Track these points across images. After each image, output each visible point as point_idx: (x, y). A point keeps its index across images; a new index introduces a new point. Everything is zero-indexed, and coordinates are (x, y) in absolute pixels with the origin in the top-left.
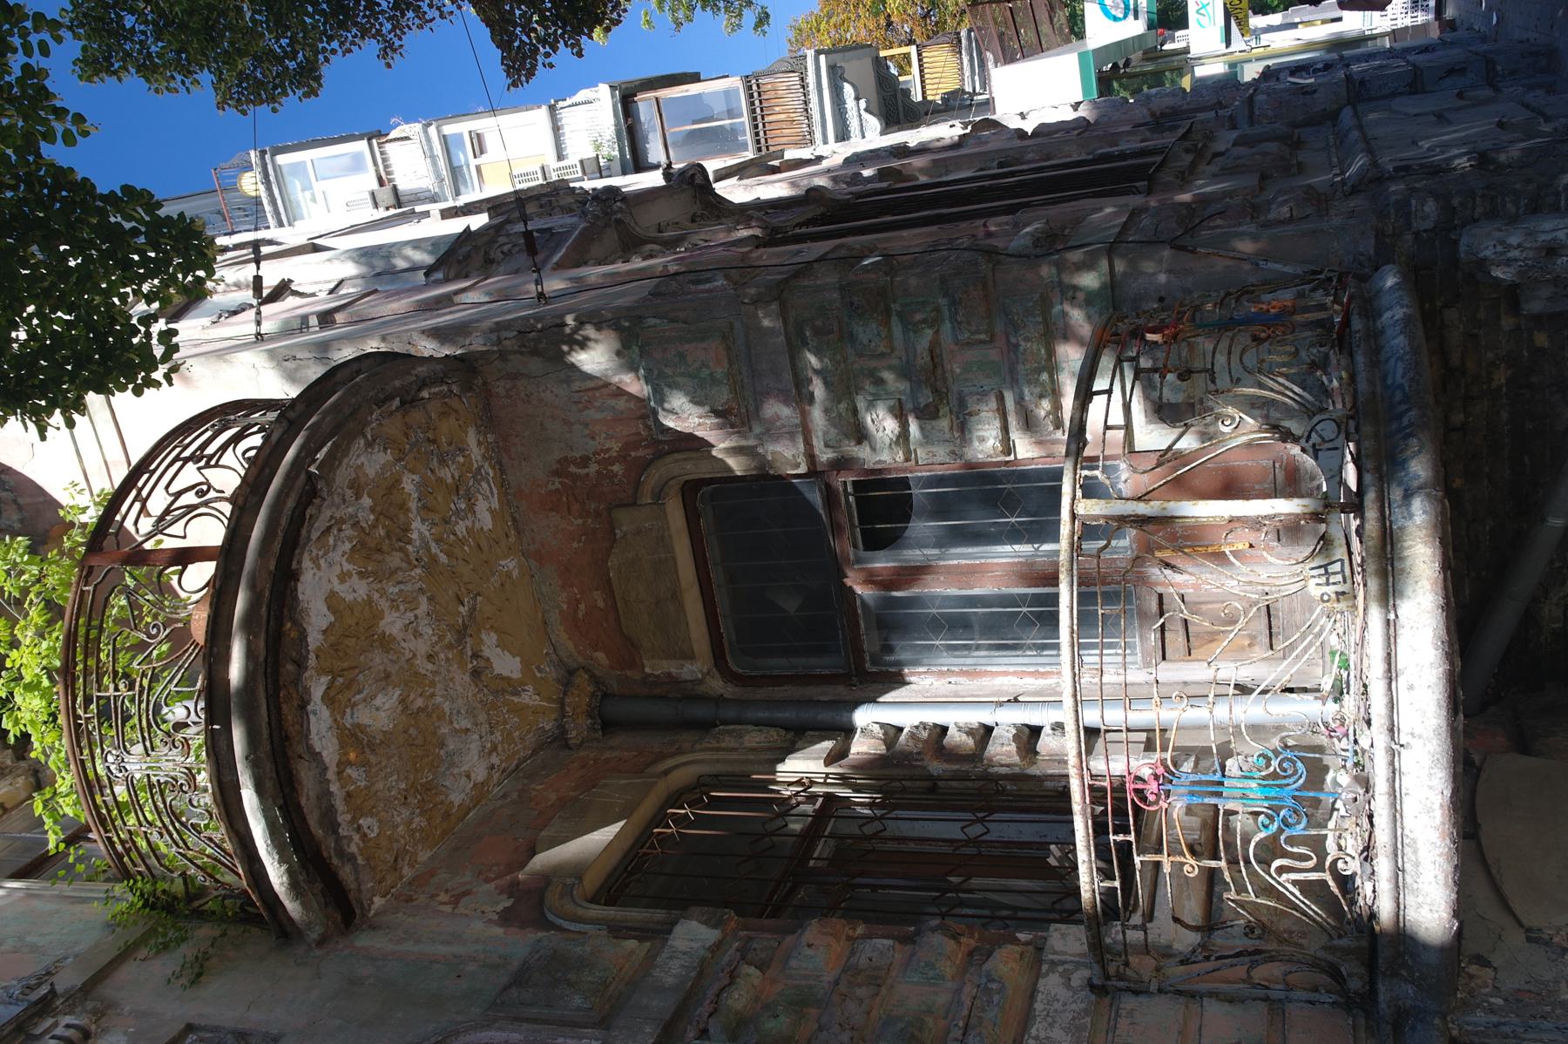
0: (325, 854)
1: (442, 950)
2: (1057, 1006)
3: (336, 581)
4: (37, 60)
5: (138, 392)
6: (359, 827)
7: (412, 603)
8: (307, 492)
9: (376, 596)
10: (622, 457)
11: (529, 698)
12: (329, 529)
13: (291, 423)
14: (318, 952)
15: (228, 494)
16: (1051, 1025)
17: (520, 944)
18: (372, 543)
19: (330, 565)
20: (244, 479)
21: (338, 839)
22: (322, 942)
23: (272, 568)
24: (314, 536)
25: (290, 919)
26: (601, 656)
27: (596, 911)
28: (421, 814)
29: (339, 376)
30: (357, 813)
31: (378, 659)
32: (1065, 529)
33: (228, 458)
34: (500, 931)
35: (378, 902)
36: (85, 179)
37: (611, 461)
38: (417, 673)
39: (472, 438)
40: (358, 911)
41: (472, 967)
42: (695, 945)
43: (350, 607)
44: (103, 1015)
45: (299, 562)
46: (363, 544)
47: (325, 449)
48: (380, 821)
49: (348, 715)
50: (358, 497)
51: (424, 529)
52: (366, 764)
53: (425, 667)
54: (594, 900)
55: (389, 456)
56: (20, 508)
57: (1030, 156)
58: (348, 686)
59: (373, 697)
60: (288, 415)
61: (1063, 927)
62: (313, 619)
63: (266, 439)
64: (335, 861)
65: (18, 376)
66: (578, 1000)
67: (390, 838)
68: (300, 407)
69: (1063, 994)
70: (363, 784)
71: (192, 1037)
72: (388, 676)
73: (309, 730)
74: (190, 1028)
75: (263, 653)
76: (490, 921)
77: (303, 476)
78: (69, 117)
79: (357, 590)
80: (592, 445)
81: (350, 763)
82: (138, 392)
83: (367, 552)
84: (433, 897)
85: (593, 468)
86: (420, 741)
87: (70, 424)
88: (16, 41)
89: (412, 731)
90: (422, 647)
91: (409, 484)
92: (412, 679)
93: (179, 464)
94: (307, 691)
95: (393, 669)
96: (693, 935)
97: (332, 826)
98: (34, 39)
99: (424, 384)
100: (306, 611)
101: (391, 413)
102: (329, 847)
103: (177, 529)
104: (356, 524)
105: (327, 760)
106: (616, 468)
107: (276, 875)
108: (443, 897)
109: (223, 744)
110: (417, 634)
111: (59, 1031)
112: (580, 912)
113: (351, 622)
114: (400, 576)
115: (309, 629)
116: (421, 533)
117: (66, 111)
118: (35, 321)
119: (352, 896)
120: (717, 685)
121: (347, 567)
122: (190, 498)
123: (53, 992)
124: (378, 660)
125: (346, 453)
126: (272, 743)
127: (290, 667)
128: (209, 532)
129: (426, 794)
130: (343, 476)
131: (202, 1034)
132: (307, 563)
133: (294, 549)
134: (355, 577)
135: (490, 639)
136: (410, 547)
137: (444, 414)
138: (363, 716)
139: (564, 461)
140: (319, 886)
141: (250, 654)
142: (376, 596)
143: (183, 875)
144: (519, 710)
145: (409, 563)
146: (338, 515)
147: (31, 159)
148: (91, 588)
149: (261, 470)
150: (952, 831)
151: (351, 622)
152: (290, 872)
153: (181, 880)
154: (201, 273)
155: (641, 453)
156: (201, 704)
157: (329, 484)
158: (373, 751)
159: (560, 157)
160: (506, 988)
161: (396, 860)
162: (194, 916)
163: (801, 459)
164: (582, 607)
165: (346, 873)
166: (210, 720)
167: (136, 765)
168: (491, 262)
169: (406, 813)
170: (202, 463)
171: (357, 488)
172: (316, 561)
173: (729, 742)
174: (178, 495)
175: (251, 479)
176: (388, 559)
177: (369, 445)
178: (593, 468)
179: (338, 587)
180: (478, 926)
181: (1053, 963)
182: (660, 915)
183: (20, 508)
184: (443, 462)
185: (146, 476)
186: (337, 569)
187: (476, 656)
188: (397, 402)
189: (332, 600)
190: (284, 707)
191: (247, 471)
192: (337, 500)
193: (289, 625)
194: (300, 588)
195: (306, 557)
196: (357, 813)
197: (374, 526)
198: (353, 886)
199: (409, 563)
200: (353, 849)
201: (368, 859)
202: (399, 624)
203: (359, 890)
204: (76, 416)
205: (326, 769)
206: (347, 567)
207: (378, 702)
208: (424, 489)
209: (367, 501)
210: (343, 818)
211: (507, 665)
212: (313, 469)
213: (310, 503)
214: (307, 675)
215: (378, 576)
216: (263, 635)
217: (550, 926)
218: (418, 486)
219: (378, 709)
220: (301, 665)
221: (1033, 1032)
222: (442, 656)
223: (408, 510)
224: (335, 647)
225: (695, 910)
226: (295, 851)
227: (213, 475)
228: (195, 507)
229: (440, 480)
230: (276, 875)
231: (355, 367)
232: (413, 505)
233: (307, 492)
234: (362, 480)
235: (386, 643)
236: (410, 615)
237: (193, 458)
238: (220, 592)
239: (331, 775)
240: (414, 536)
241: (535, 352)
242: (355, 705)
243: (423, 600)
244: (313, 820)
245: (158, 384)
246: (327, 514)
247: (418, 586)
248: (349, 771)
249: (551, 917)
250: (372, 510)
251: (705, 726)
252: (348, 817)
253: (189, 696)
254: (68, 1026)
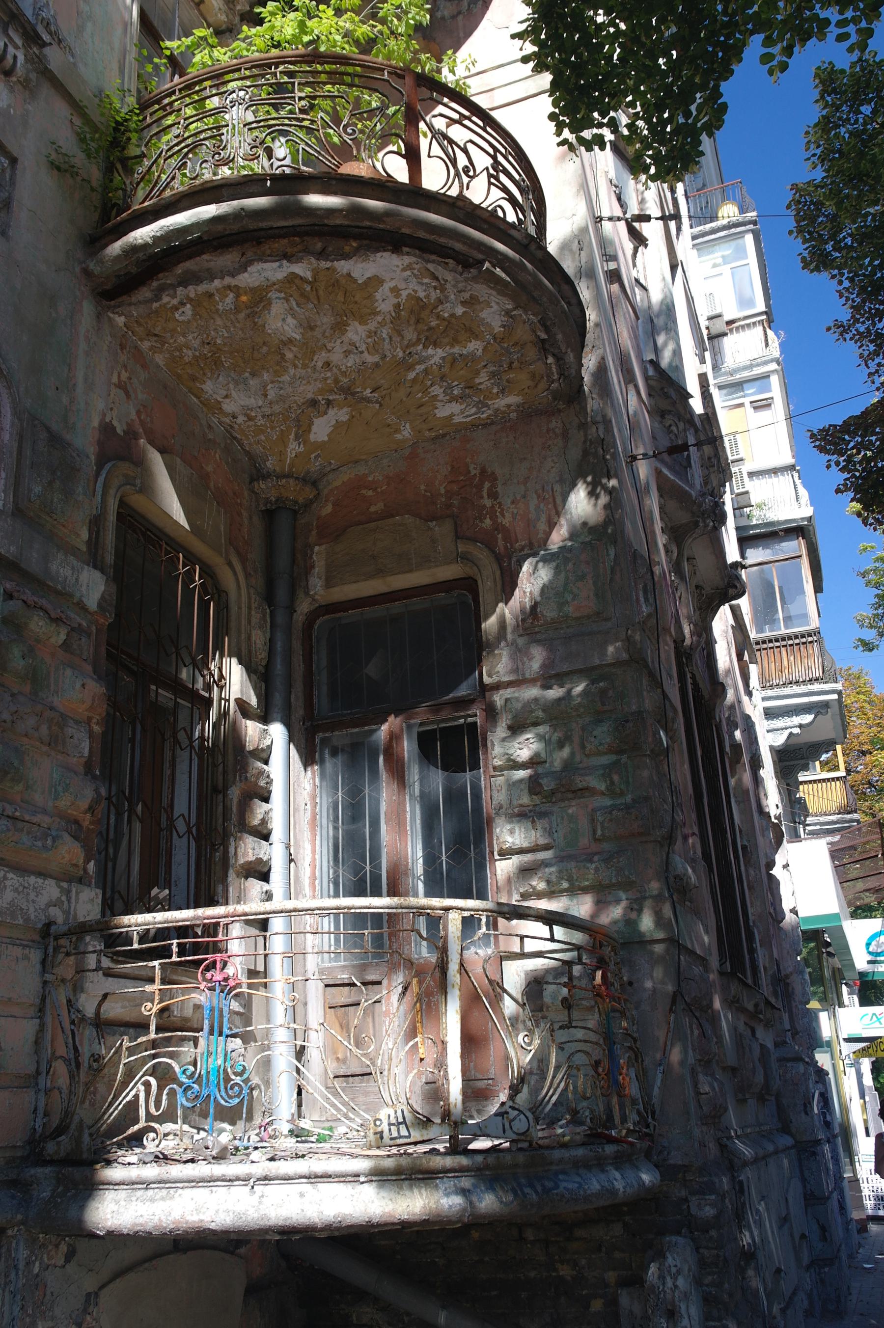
0: (161, 275)
1: (80, 375)
2: (32, 896)
3: (392, 284)
4: (833, 31)
5: (552, 117)
6: (183, 304)
7: (374, 348)
8: (468, 259)
9: (379, 318)
10: (498, 527)
11: (293, 448)
12: (437, 279)
13: (526, 247)
14: (77, 269)
15: (466, 193)
16: (16, 890)
17: (85, 440)
18: (424, 314)
19: (406, 280)
20: (478, 207)
21: (174, 287)
22: (87, 273)
23: (404, 230)
24: (431, 266)
25: (107, 245)
26: (329, 509)
27: (113, 506)
28: (194, 356)
29: (565, 287)
30: (196, 303)
31: (326, 320)
32: (436, 902)
33: (496, 193)
34: (96, 423)
35: (121, 320)
36: (732, 72)
37: (494, 518)
38: (314, 353)
39: (513, 399)
40: (113, 303)
41: (65, 400)
42: (84, 589)
43: (370, 297)
44: (25, 87)
45: (408, 254)
46: (424, 307)
47: (503, 275)
48: (189, 322)
49: (278, 295)
50: (464, 303)
51: (436, 359)
52: (237, 310)
53: (320, 359)
54: (122, 503)
55: (498, 329)
56: (454, 17)
57: (752, 872)
58: (303, 295)
59: (294, 316)
60: (532, 243)
61: (99, 900)
62: (360, 265)
63: (512, 225)
64: (155, 284)
65: (565, 15)
66: (37, 489)
67: (174, 331)
68: (539, 254)
69: (43, 900)
70: (220, 307)
71: (6, 163)
72: (312, 328)
73: (266, 261)
74: (14, 161)
75: (331, 222)
76: (104, 415)
77: (480, 256)
78: (784, 59)
79: (385, 303)
80: (507, 502)
81: (238, 296)
82: (552, 117)
83: (416, 311)
84: (125, 367)
85: (488, 503)
86: (257, 356)
87: (525, 60)
88: (849, 14)
89: (265, 349)
90: (336, 357)
91: (474, 346)
92: (309, 349)
93: (491, 151)
94: (299, 260)
95: (317, 333)
96: (93, 587)
97: (185, 281)
98: (851, 29)
99: (559, 359)
100: (367, 259)
101: (534, 331)
103: (436, 150)
104: (440, 302)
105: (240, 277)
106: (488, 521)
107: (143, 234)
108: (124, 375)
109: (254, 189)
110: (347, 353)
111: (11, 50)
112: (112, 492)
113: (358, 298)
114: (397, 339)
115: (351, 262)
116: (432, 356)
117: (790, 56)
118: (612, 30)
119: (125, 298)
120: (304, 607)
121: (404, 294)
122: (462, 161)
123: (44, 44)
124: (325, 320)
125: (501, 293)
126: (255, 230)
127: (319, 246)
128: (434, 177)
129: (211, 361)
130: (482, 290)
131: (8, 171)
132: (407, 260)
133: (420, 249)
134: (396, 301)
135: (342, 414)
136: (421, 347)
137: (533, 376)
138: (278, 307)
139: (493, 478)
140: (134, 270)
141: (330, 212)
142: (379, 318)
143: (143, 155)
144: (283, 439)
145: (407, 347)
146: (448, 286)
147: (750, 26)
148: (386, 77)
149: (485, 221)
150: (181, 806)
151: (358, 298)
152: (145, 246)
153: (138, 153)
154: (653, 170)
155: (501, 543)
156: (288, 171)
157: (474, 279)
158: (248, 316)
159: (751, 475)
160: (48, 429)
161: (156, 335)
162: (109, 163)
163: (495, 679)
164: (370, 493)
165: (145, 293)
166: (274, 178)
167: (236, 115)
169: (196, 343)
170: (492, 171)
171: (471, 302)
172: (409, 267)
173: (256, 617)
174: (465, 151)
175: (478, 212)
176: (411, 329)
177: (508, 313)
178: (488, 503)
179: (387, 286)
180: (101, 405)
181: (69, 891)
182: (109, 559)
183: (454, 17)
184: (493, 375)
185: (481, 123)
186: (402, 285)
187: (329, 403)
188: (544, 336)
189: (376, 281)
190: (286, 241)
191: (486, 210)
192: (461, 285)
193: (355, 244)
194: (386, 254)
195: (414, 259)
196: (196, 303)
197: (438, 317)
198: (134, 299)
199: (407, 347)
200: (166, 299)
201: (157, 311)
202: (355, 338)
203: (130, 304)
204: (531, 64)
205: (233, 276)
206: (404, 294)
207: (290, 320)
208: (469, 360)
209: (460, 310)
210: (191, 291)
212: (487, 265)
213: (458, 262)
214: (313, 260)
215: (396, 320)
216: (346, 223)
217: (100, 466)
218: (473, 354)
219: (284, 320)
220: (321, 255)
221: (10, 875)
222: (329, 374)
223: (452, 346)
224: (336, 284)
225: (113, 589)
226: (163, 250)
227: (481, 181)
228: (455, 165)
229: (477, 373)
230: (143, 234)
231: (574, 301)
232: (456, 350)
233: (468, 259)
234: (478, 307)
235: (340, 327)
236: (363, 347)
237: (496, 164)
238: (382, 186)
239: (228, 280)
240: (430, 351)
241: (586, 453)
242: (287, 301)
243: (376, 358)
244: (189, 265)
245: (559, 133)
246: (449, 276)
247: (388, 354)
248: (231, 295)
249: (108, 466)
250: (452, 315)
251: (269, 597)
252: (192, 295)
253: (295, 160)
254: (15, 57)
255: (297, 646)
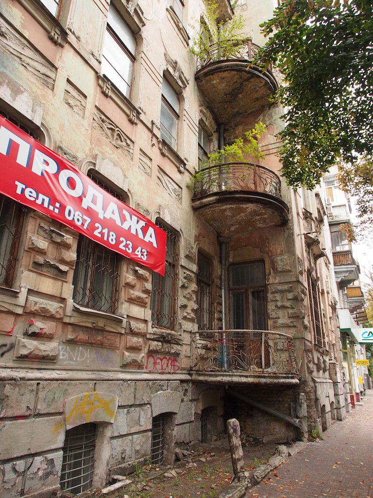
10: (269, 250)
11: (227, 231)
39: (273, 224)
57: (325, 320)
85: (267, 245)
93: (270, 178)
96: (194, 268)
97: (211, 208)
102: (207, 207)
106: (267, 249)
122: (265, 182)
138: (228, 211)
139: (268, 239)
150: (205, 307)
159: (333, 207)
163: (268, 283)
168: (306, 219)
178: (267, 245)
182: (197, 261)
189: (248, 207)
211: (232, 229)
255: (226, 272)
